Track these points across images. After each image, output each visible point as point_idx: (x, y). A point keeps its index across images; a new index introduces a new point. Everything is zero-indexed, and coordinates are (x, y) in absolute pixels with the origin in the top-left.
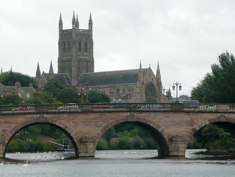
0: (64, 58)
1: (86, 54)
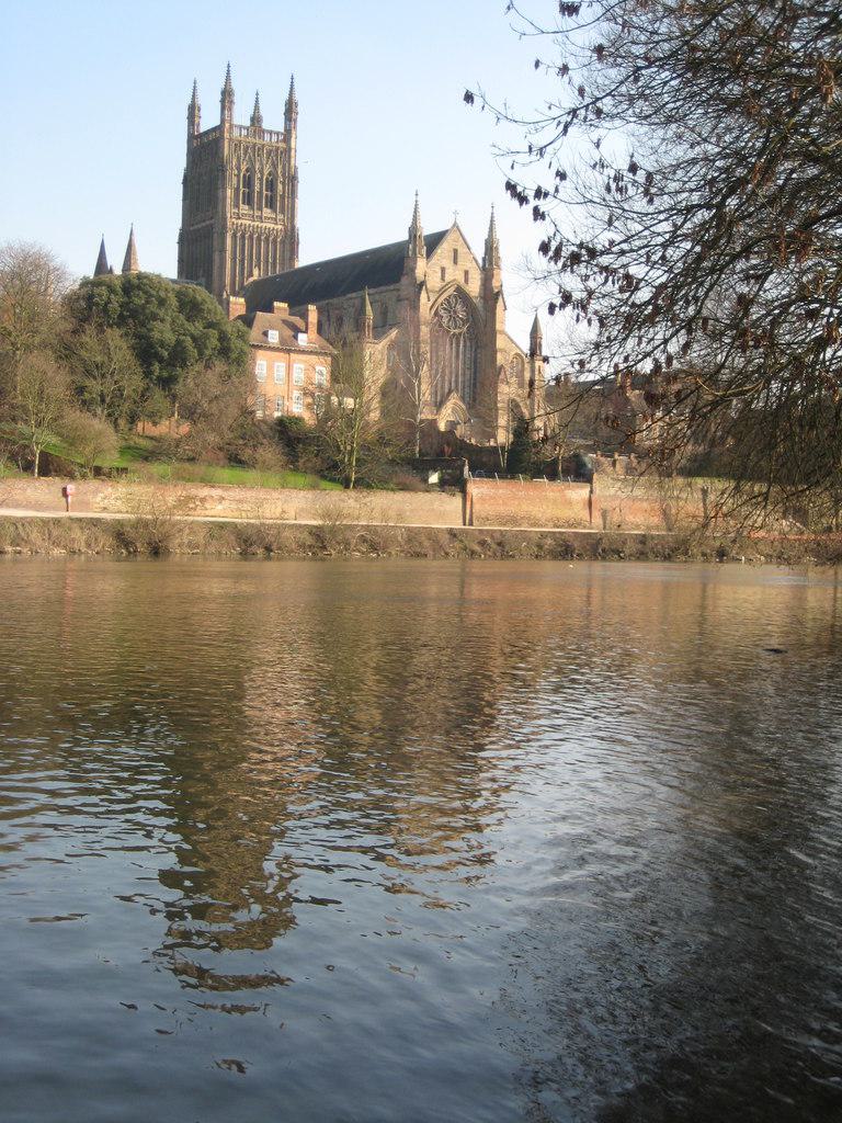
0: (196, 227)
1: (267, 212)
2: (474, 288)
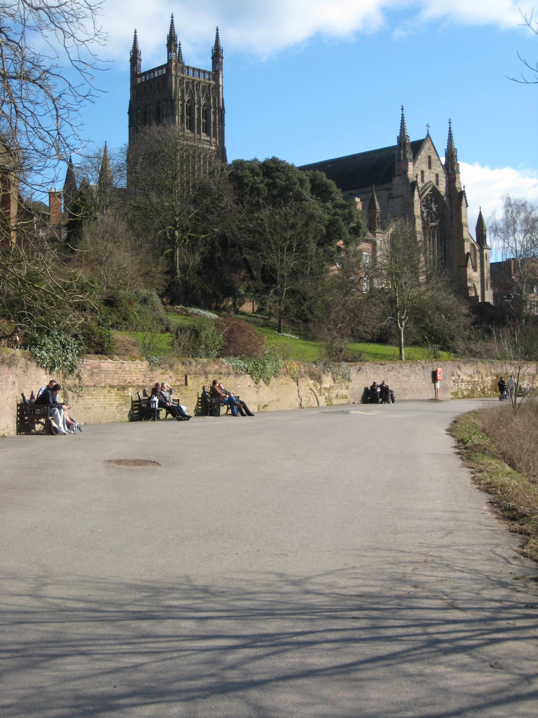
2: (442, 188)
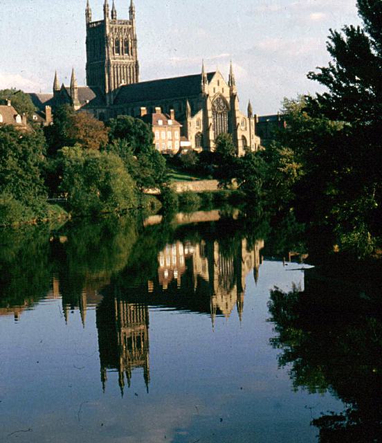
2: (227, 95)
